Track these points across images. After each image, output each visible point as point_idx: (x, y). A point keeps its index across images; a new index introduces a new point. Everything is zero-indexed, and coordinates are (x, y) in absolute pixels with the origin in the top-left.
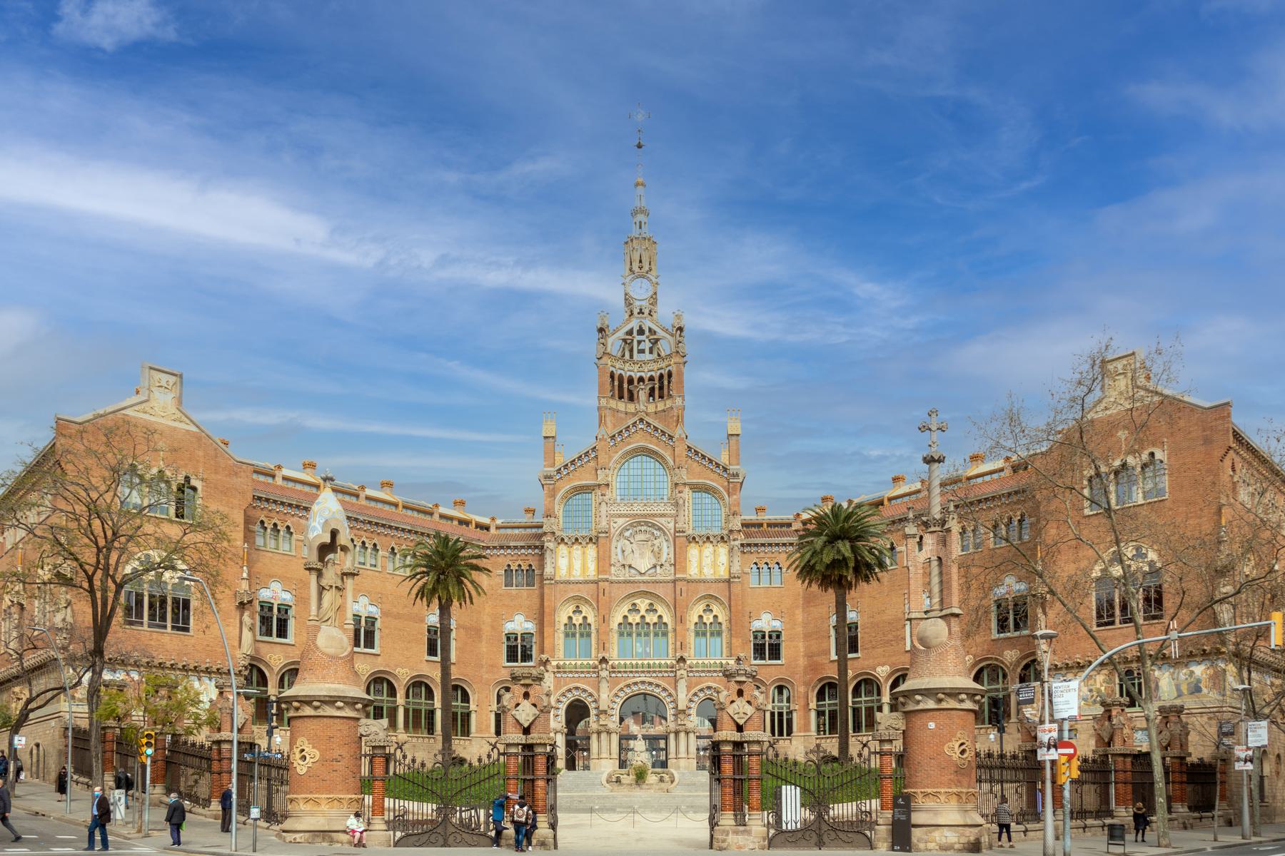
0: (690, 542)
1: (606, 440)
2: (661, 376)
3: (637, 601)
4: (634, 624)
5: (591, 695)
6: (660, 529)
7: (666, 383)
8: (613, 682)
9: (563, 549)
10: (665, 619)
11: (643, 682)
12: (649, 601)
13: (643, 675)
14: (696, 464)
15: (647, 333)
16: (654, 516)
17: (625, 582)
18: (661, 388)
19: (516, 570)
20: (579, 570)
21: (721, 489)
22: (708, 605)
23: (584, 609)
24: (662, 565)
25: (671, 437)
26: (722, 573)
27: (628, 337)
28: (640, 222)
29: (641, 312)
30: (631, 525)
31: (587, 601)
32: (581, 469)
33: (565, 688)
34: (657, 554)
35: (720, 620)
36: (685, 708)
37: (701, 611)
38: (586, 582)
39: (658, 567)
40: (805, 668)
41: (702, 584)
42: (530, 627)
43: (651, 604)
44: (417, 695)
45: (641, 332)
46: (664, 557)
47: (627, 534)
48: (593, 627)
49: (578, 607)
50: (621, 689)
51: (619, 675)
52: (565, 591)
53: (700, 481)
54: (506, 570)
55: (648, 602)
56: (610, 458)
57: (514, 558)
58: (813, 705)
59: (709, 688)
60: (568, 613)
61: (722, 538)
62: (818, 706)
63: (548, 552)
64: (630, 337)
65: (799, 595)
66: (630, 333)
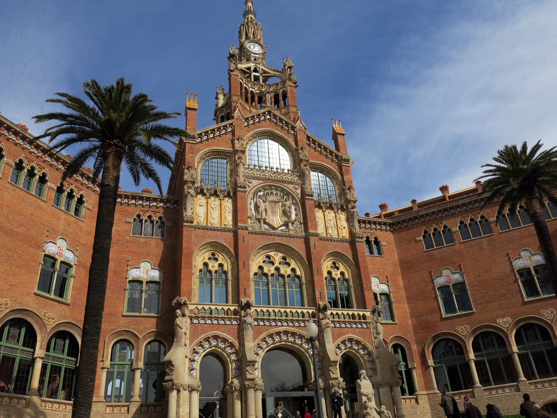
0: (316, 207)
1: (241, 120)
3: (272, 254)
5: (232, 345)
6: (288, 194)
8: (257, 331)
9: (201, 199)
10: (298, 273)
11: (286, 333)
13: (285, 324)
14: (313, 150)
16: (284, 182)
17: (262, 234)
19: (146, 221)
20: (217, 219)
21: (335, 170)
24: (293, 223)
25: (293, 128)
26: (344, 235)
29: (255, 60)
31: (223, 249)
32: (219, 138)
33: (203, 336)
34: (285, 213)
40: (414, 327)
41: (330, 243)
42: (155, 274)
43: (284, 258)
44: (13, 337)
46: (293, 217)
47: (261, 193)
48: (230, 274)
50: (264, 340)
52: (205, 237)
53: (318, 162)
54: (135, 220)
55: (280, 255)
56: (245, 135)
57: (145, 209)
58: (431, 362)
59: (350, 340)
60: (204, 258)
63: (189, 196)
64: (249, 72)
65: (397, 265)
66: (249, 69)
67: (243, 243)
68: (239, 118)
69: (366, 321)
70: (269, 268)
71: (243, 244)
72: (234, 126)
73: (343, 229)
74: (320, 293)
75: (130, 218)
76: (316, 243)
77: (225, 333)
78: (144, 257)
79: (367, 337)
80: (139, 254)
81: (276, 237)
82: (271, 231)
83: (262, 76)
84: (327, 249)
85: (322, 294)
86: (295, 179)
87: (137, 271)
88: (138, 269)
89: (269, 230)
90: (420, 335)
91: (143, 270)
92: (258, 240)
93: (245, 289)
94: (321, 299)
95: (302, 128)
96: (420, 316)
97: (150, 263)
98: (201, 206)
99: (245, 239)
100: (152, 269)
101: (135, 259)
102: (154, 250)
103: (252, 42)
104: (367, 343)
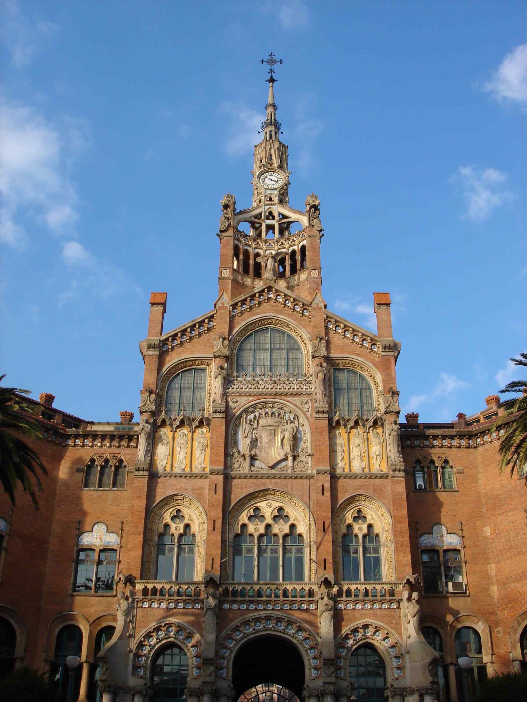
2: (294, 252)
4: (256, 536)
7: (298, 257)
12: (276, 505)
16: (286, 394)
23: (186, 511)
27: (256, 220)
28: (271, 131)
30: (255, 406)
35: (377, 530)
36: (333, 656)
38: (192, 476)
39: (290, 459)
43: (280, 509)
45: (271, 215)
47: (251, 416)
51: (235, 606)
61: (375, 422)
67: (215, 493)
68: (223, 306)
69: (394, 598)
71: (215, 495)
73: (375, 457)
81: (268, 481)
82: (262, 472)
83: (279, 224)
84: (347, 492)
86: (304, 387)
87: (88, 536)
88: (90, 534)
89: (258, 469)
100: (107, 532)
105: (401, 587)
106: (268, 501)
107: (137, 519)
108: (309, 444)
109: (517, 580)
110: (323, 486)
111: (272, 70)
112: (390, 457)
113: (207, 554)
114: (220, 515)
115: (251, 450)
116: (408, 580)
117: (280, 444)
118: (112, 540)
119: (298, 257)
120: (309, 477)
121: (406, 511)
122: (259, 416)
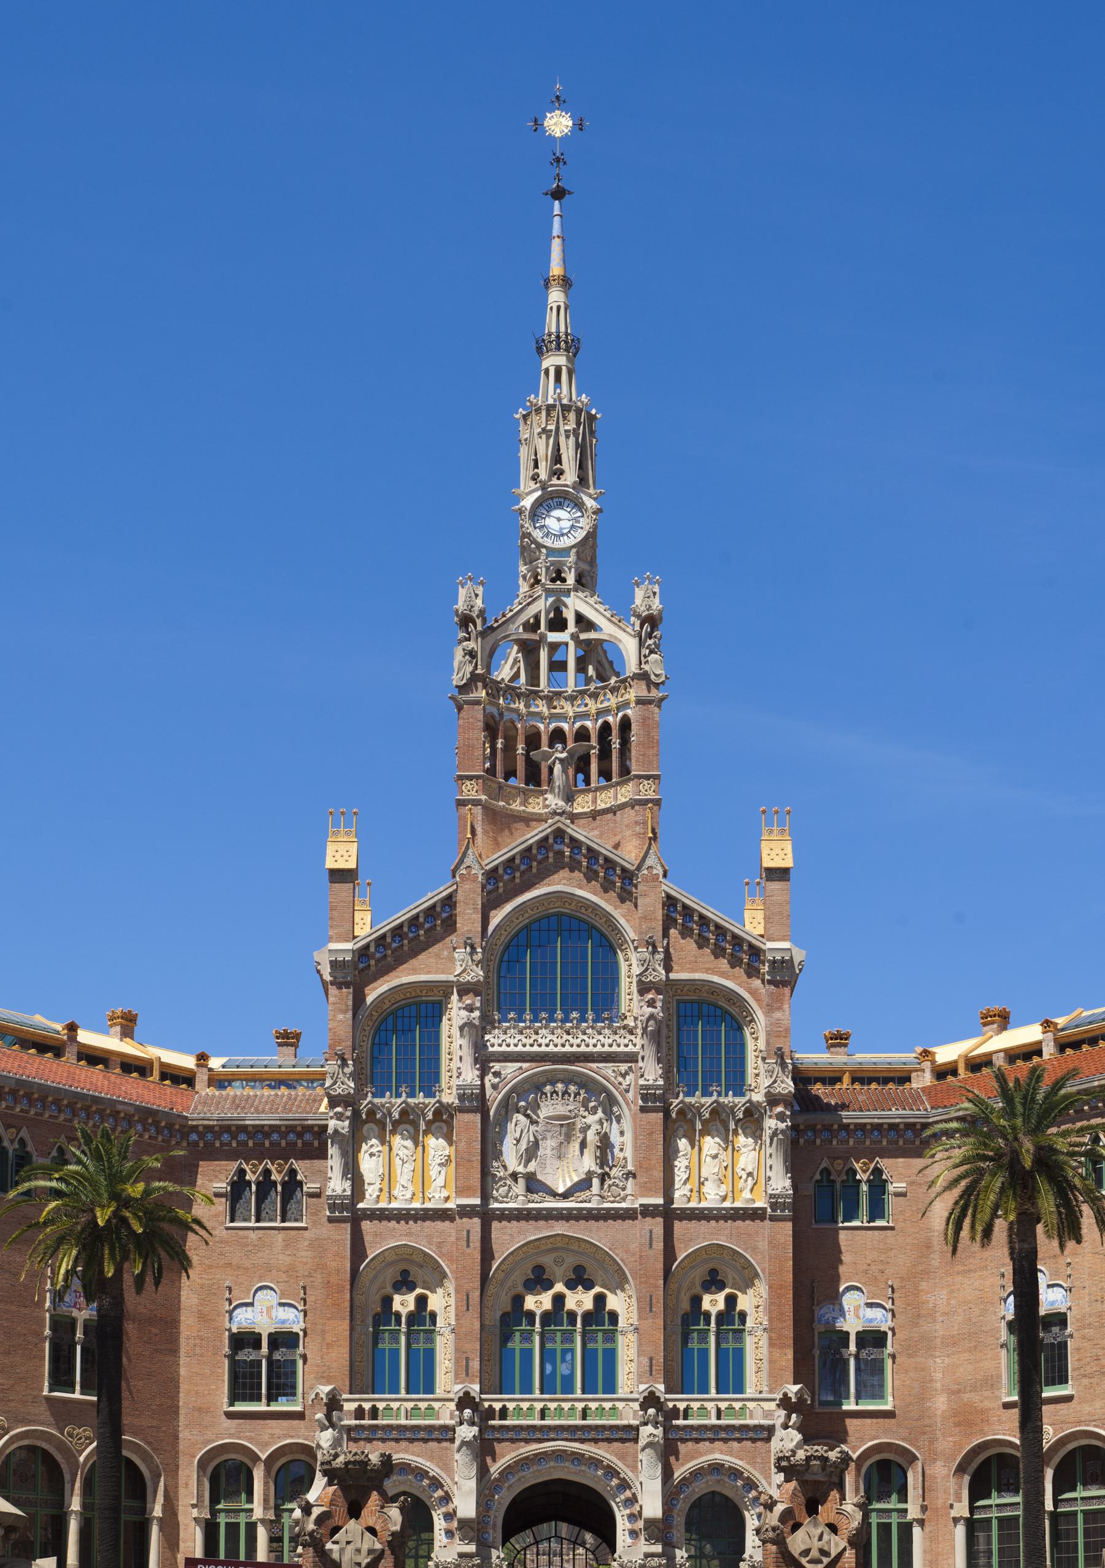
2: (606, 728)
4: (538, 1312)
7: (616, 743)
11: (559, 1455)
12: (571, 1261)
15: (572, 627)
16: (588, 1058)
18: (605, 754)
22: (713, 1272)
37: (698, 1283)
39: (596, 1182)
49: (405, 1273)
59: (716, 1468)
62: (972, 1509)
65: (928, 1246)
67: (468, 1246)
68: (469, 873)
70: (538, 1297)
71: (468, 1251)
72: (456, 902)
73: (744, 1177)
74: (651, 1359)
75: (221, 1181)
76: (654, 1231)
77: (422, 1456)
78: (260, 1277)
79: (759, 1460)
80: (246, 1269)
85: (654, 1362)
90: (951, 1439)
91: (260, 1307)
92: (509, 1231)
93: (467, 1359)
94: (651, 1374)
95: (655, 872)
96: (959, 1391)
97: (272, 1289)
98: (371, 1155)
99: (471, 1238)
101: (241, 1283)
102: (281, 1257)
103: (552, 499)
104: (757, 1475)
105: (772, 1406)
106: (557, 1254)
107: (338, 1293)
108: (628, 1153)
109: (974, 1389)
110: (651, 1232)
111: (558, 160)
112: (770, 1178)
113: (457, 1350)
114: (478, 1284)
115: (526, 1166)
116: (785, 1394)
117: (578, 1152)
118: (291, 1319)
119: (616, 743)
120: (628, 1215)
121: (789, 1277)
122: (541, 1098)
